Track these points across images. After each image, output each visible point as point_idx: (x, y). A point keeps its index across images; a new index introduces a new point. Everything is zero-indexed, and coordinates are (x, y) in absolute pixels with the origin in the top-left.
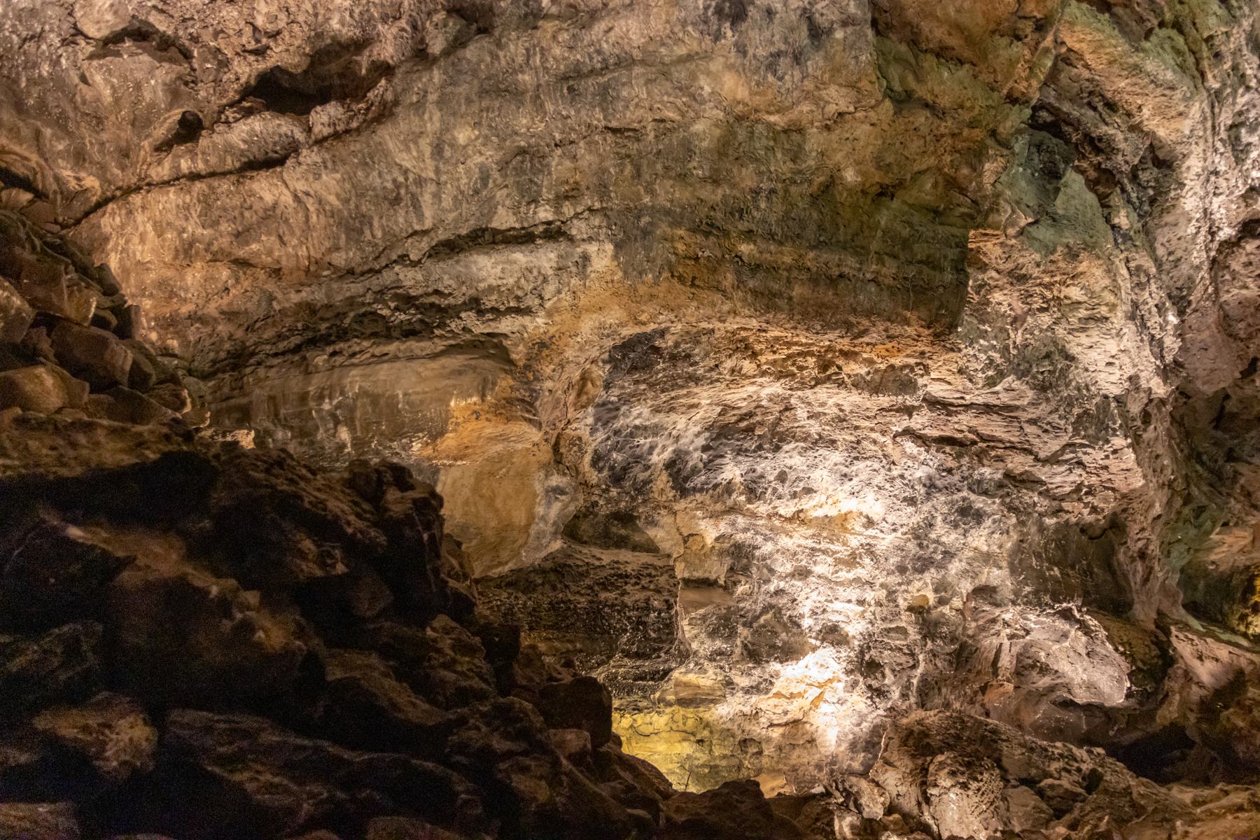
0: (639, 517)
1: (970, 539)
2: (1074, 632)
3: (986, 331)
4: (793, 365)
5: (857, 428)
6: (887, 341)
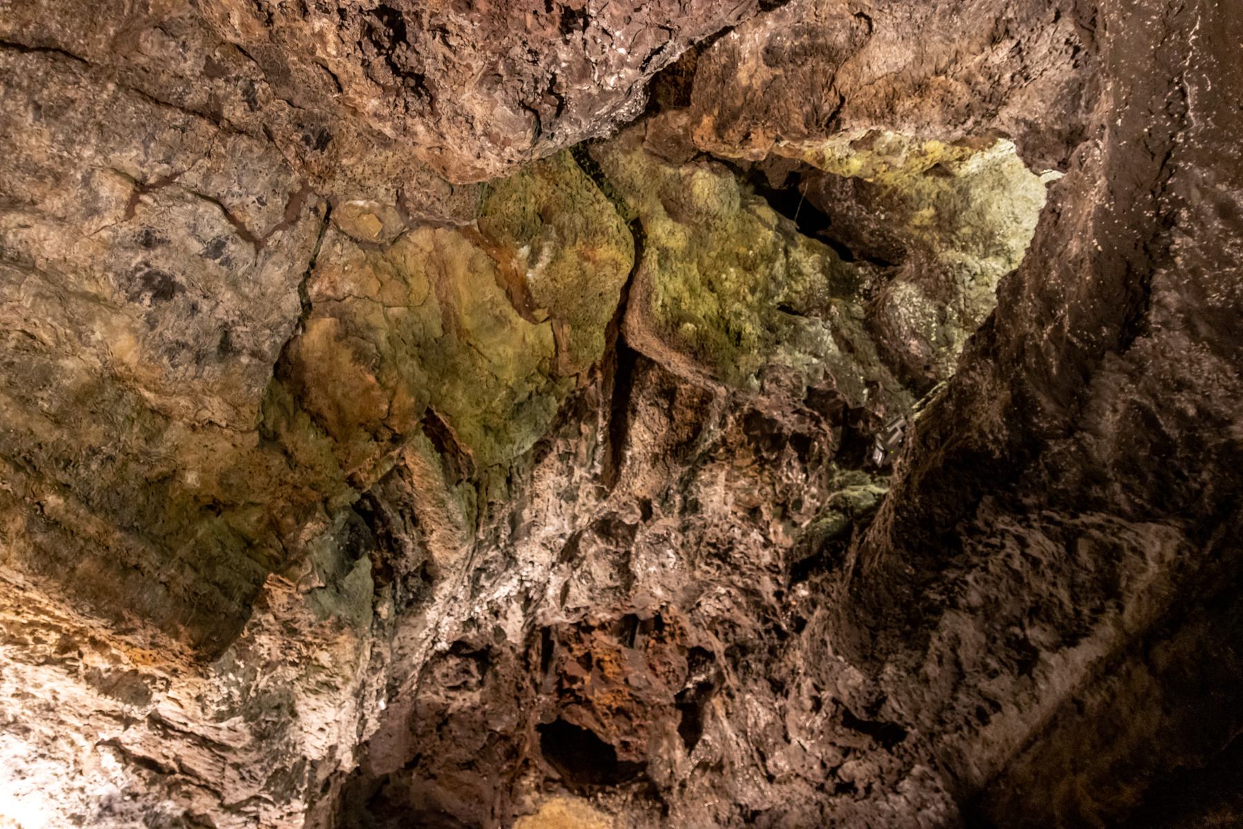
3: (239, 667)
4: (32, 634)
5: (61, 722)
6: (148, 647)
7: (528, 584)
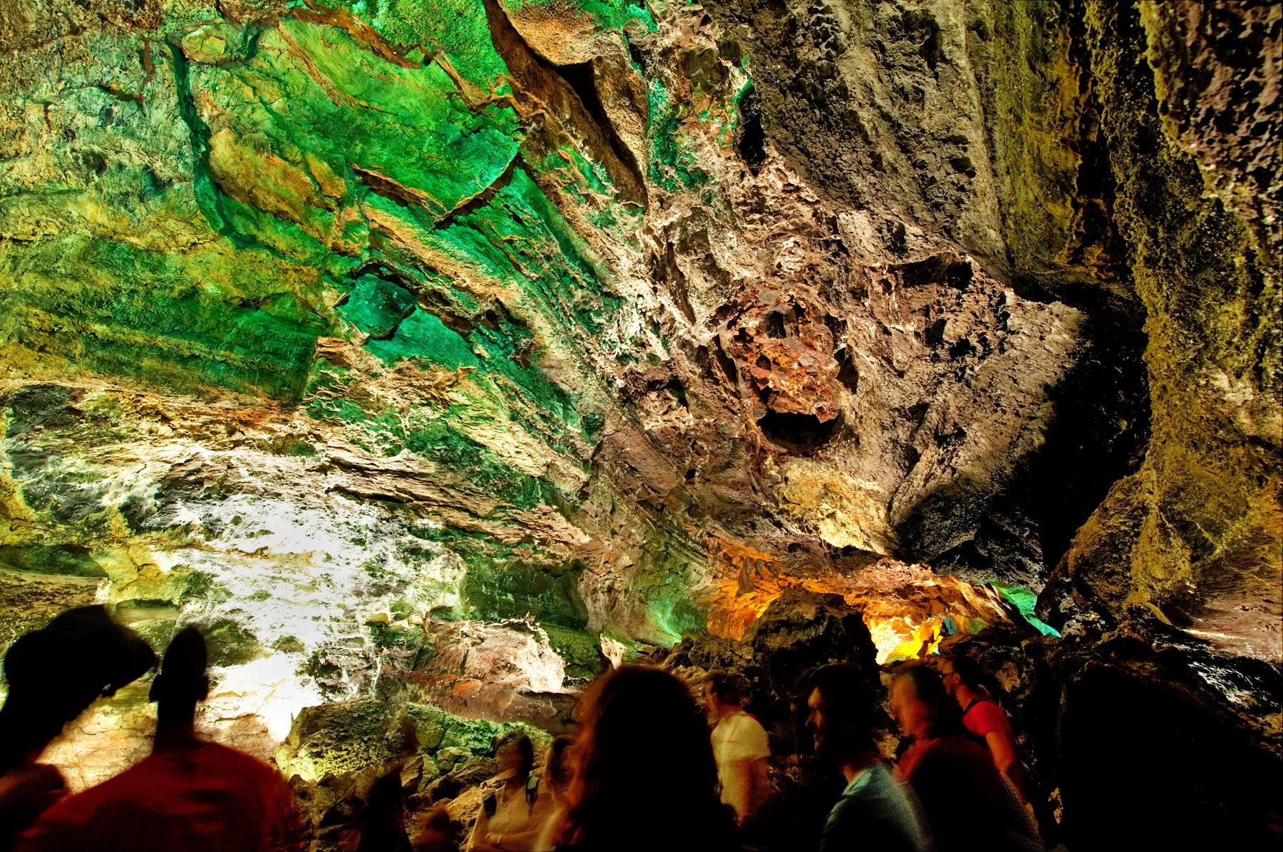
0: (91, 550)
1: (423, 572)
2: (530, 639)
5: (296, 484)
7: (649, 314)
